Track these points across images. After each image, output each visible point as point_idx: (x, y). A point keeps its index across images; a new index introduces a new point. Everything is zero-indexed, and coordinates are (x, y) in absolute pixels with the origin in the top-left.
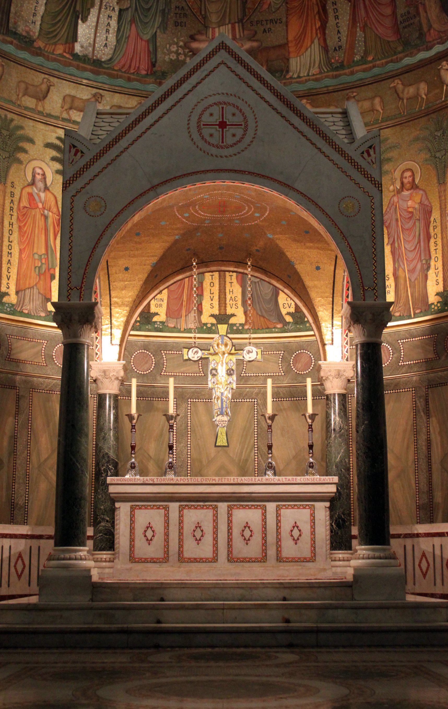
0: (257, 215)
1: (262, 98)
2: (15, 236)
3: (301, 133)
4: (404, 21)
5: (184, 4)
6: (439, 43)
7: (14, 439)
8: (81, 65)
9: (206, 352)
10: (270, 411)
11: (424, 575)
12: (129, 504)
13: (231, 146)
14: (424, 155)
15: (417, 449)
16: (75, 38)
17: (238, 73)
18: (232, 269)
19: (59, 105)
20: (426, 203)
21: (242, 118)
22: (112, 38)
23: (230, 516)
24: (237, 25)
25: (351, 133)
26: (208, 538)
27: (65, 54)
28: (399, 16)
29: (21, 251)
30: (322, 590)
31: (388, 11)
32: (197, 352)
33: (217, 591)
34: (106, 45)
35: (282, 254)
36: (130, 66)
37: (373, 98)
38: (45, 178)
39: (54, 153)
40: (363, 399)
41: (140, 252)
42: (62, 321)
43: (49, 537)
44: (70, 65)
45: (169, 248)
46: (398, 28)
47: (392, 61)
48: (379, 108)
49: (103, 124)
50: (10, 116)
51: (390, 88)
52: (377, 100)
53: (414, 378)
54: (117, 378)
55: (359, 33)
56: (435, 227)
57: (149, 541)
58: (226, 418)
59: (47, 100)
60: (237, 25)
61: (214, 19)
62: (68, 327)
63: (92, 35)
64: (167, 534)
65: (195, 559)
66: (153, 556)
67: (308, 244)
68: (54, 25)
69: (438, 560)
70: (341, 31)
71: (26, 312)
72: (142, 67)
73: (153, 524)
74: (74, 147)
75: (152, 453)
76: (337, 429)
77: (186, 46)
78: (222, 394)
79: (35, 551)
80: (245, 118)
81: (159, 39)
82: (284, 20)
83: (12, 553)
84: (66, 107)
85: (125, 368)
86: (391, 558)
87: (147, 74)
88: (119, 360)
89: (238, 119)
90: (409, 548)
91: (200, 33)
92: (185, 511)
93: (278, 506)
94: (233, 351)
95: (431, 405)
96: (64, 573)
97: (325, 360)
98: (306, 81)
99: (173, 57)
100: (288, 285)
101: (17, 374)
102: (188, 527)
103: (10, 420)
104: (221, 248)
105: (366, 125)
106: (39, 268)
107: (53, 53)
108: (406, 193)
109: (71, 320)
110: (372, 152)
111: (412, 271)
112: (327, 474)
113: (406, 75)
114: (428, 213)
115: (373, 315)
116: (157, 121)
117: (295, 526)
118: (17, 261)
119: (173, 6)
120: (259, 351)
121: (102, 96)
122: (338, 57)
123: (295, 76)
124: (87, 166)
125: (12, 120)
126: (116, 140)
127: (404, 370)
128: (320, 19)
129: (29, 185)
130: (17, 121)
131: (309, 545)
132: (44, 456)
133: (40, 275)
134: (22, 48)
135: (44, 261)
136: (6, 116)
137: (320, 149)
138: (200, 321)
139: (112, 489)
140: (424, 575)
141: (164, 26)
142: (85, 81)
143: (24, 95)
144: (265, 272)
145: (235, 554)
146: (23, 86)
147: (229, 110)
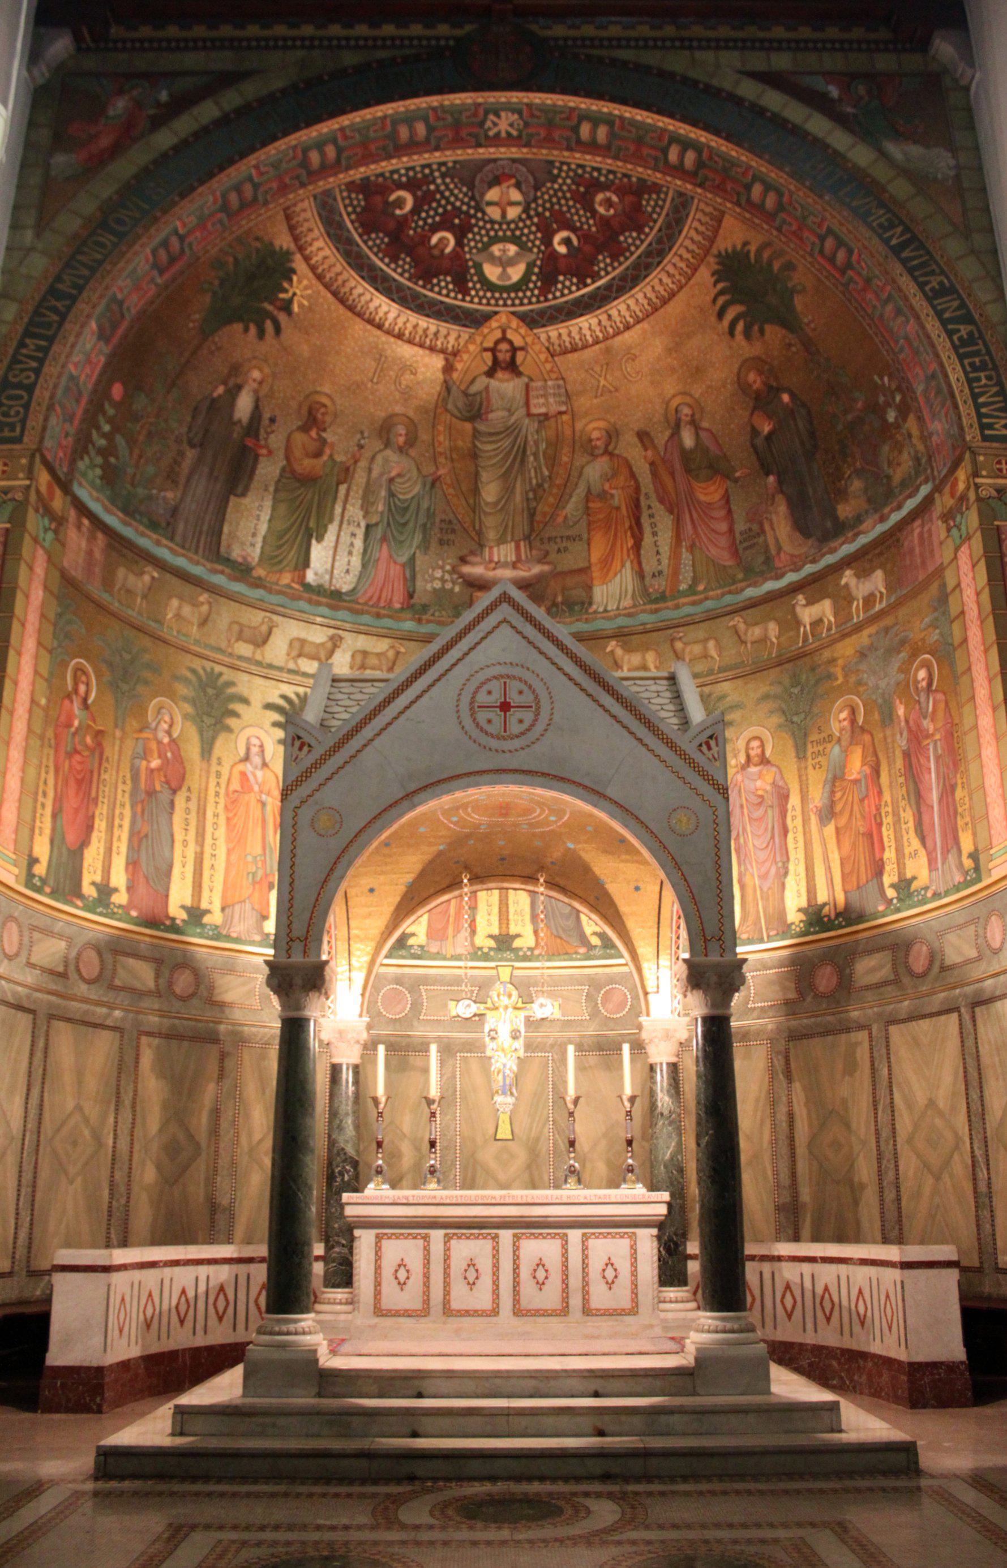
0: (552, 818)
1: (560, 669)
2: (222, 830)
3: (614, 717)
4: (745, 540)
5: (451, 516)
6: (793, 571)
7: (216, 1113)
8: (314, 597)
9: (482, 1006)
10: (571, 1092)
11: (789, 1316)
12: (374, 1232)
13: (517, 737)
14: (776, 719)
15: (774, 1126)
16: (307, 564)
17: (526, 634)
18: (517, 886)
19: (284, 652)
20: (781, 783)
21: (531, 697)
22: (356, 561)
23: (516, 1249)
24: (522, 543)
25: (681, 709)
26: (486, 1280)
27: (294, 585)
28: (737, 535)
29: (229, 852)
30: (650, 1379)
31: (723, 527)
32: (468, 1006)
33: (498, 1381)
34: (348, 571)
35: (587, 869)
36: (379, 598)
37: (705, 641)
38: (263, 751)
39: (277, 717)
40: (707, 1098)
41: (388, 868)
42: (279, 986)
43: (262, 1260)
44: (300, 598)
45: (431, 862)
46: (737, 551)
47: (730, 592)
48: (713, 653)
49: (340, 696)
50: (218, 669)
51: (728, 628)
52: (711, 644)
53: (770, 1027)
54: (358, 1042)
55: (686, 556)
56: (794, 818)
57: (402, 1285)
58: (510, 1100)
59: (267, 647)
60: (522, 543)
61: (491, 535)
62: (287, 995)
63: (330, 560)
64: (427, 1276)
65: (467, 1311)
66: (407, 1306)
67: (624, 857)
68: (280, 547)
69: (808, 1295)
70: (661, 551)
71: (234, 935)
72: (395, 599)
73: (406, 1261)
74: (299, 738)
75: (406, 1127)
76: (666, 1112)
77: (454, 570)
78: (505, 1065)
79: (242, 1281)
80: (537, 697)
81: (418, 562)
82: (585, 536)
83: (211, 1284)
84: (294, 653)
85: (369, 1027)
86: (748, 1331)
87: (402, 609)
88: (361, 1016)
89: (528, 698)
90: (767, 1276)
91: (472, 553)
92: (453, 1242)
93: (584, 1235)
94: (520, 1005)
95: (793, 1065)
96: (277, 1355)
97: (648, 1015)
98: (616, 616)
99: (438, 585)
100: (594, 908)
101: (220, 1023)
102: (457, 1265)
103: (211, 1087)
104: (503, 859)
105: (695, 676)
106: (254, 874)
107: (277, 584)
108: (753, 769)
109: (291, 986)
110: (712, 743)
111: (764, 877)
112: (652, 1187)
113: (749, 611)
114: (784, 797)
115: (720, 976)
116: (413, 702)
117: (609, 1263)
118: (223, 865)
119: (437, 520)
120: (556, 1004)
121: (341, 638)
122: (660, 585)
123: (601, 609)
124: (316, 765)
125: (221, 674)
126: (357, 729)
127: (755, 1014)
128: (633, 536)
129: (241, 761)
130: (228, 675)
131: (628, 1292)
132: (257, 1136)
133: (254, 883)
134: (236, 579)
135: (260, 865)
136: (212, 669)
137: (640, 740)
138: (472, 944)
139: (349, 1211)
140: (789, 1316)
141: (425, 545)
142: (319, 620)
143: (237, 640)
144: (563, 890)
145: (524, 1304)
146: (236, 628)
147: (514, 686)
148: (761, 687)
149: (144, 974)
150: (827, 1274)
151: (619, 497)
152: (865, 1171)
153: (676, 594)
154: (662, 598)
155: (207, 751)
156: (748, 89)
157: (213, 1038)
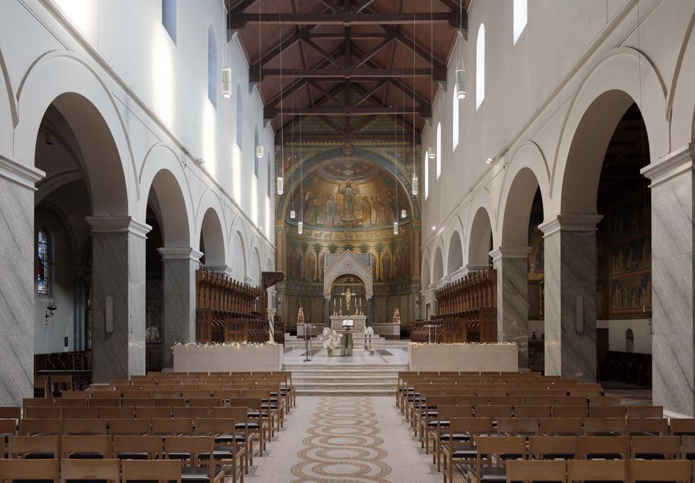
156: (386, 156)
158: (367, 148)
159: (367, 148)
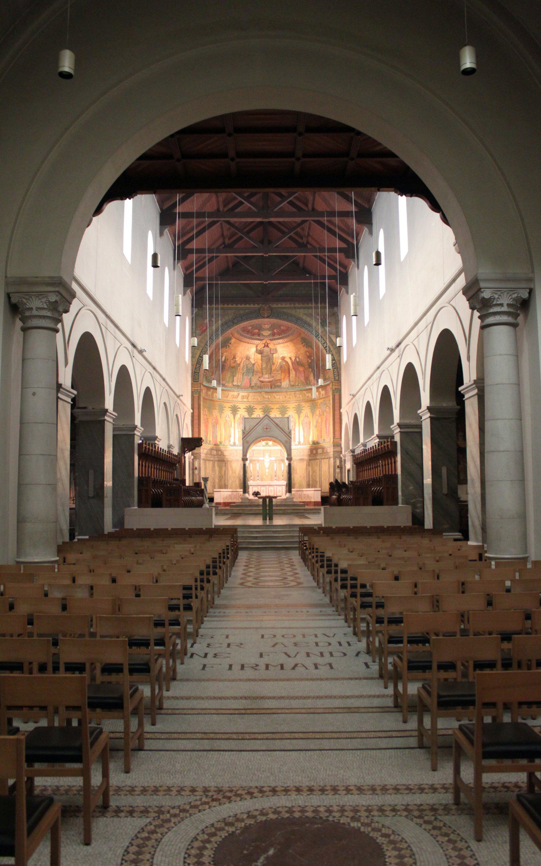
61: (264, 373)
114: (310, 423)
122: (292, 383)
148: (308, 404)
149: (214, 452)
150: (308, 492)
151: (286, 368)
152: (318, 479)
153: (296, 385)
154: (293, 386)
155: (221, 417)
156: (304, 317)
157: (223, 461)
158: (285, 310)
159: (285, 310)
